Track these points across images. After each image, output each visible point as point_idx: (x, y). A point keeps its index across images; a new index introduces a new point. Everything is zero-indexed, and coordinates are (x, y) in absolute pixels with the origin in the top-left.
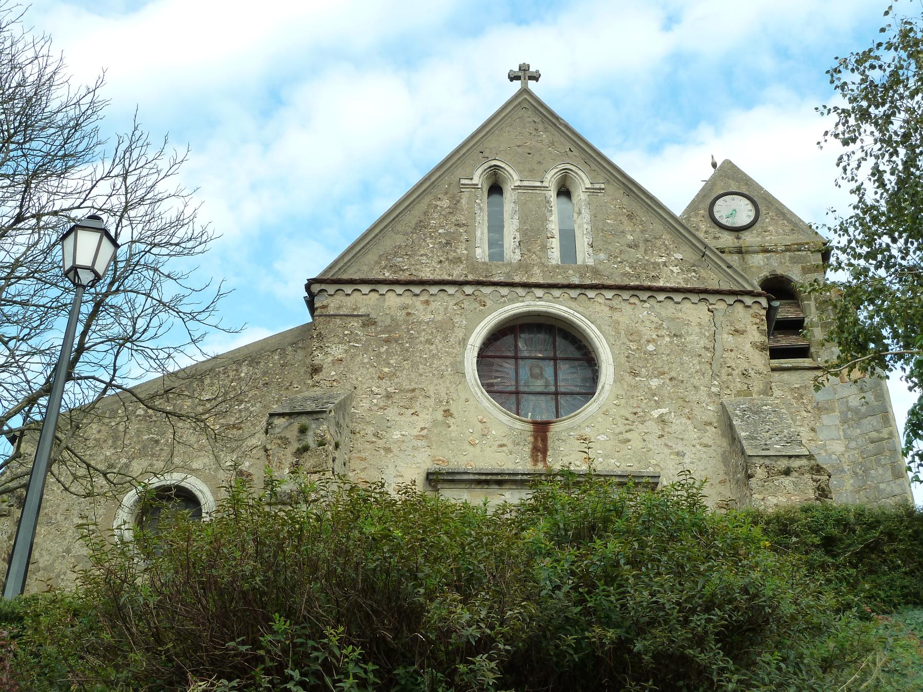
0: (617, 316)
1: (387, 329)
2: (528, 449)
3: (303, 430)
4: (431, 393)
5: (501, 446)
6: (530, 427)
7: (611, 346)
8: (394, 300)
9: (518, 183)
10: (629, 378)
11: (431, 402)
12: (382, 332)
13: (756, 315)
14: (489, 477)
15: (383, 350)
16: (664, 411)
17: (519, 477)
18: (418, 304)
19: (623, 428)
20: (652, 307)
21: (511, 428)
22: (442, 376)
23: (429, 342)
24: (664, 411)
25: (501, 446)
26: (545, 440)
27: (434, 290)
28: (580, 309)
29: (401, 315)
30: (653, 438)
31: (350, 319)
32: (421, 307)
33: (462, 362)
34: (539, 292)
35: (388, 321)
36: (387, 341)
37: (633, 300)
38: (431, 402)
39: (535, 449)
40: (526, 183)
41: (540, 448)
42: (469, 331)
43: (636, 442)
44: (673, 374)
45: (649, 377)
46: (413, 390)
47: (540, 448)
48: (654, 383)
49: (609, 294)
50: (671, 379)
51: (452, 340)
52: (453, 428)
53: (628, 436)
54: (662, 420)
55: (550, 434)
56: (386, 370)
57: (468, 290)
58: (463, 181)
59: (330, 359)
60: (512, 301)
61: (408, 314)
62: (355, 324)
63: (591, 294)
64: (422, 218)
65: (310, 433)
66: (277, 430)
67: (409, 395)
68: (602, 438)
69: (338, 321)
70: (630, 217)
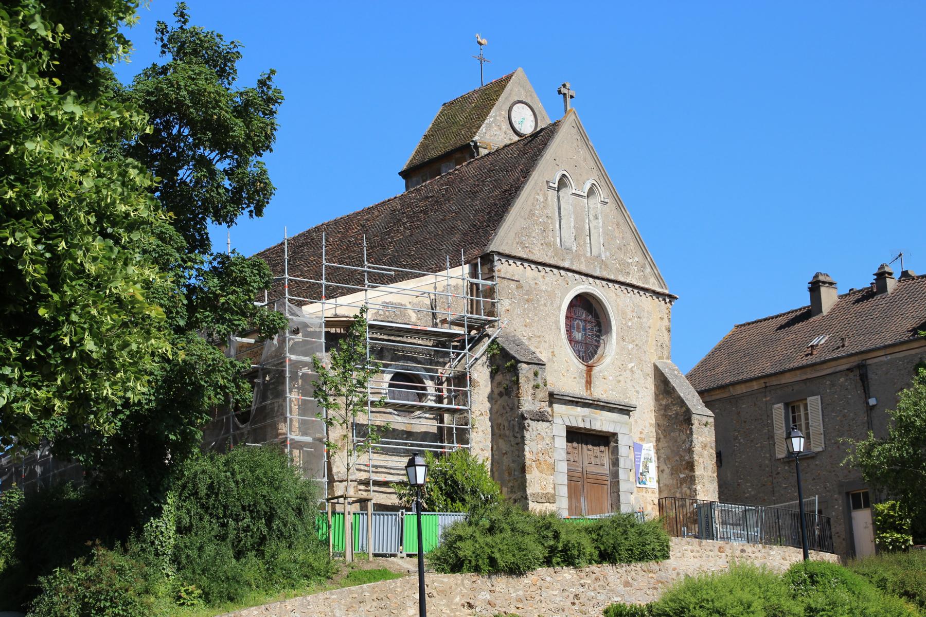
0: (618, 300)
1: (528, 293)
2: (584, 381)
3: (536, 374)
4: (547, 339)
5: (575, 378)
6: (585, 368)
7: (616, 320)
8: (529, 273)
9: (574, 191)
10: (621, 342)
11: (546, 345)
12: (526, 294)
13: (668, 308)
14: (580, 400)
15: (527, 306)
16: (633, 364)
17: (587, 401)
18: (540, 277)
19: (618, 374)
20: (631, 297)
21: (578, 368)
22: (551, 330)
23: (545, 305)
24: (633, 364)
25: (575, 378)
26: (590, 377)
27: (548, 269)
28: (605, 294)
29: (532, 283)
30: (628, 381)
31: (511, 282)
32: (541, 280)
33: (559, 321)
34: (591, 280)
35: (527, 288)
36: (528, 301)
37: (625, 291)
38: (546, 345)
39: (587, 382)
40: (577, 192)
41: (589, 383)
42: (562, 299)
43: (622, 383)
44: (637, 342)
45: (629, 343)
46: (539, 337)
47: (589, 383)
48: (630, 346)
49: (617, 286)
50: (637, 345)
51: (555, 306)
52: (556, 364)
53: (620, 378)
54: (632, 371)
55: (592, 373)
56: (528, 321)
57: (562, 272)
58: (551, 185)
59: (504, 309)
60: (579, 284)
61: (536, 284)
62: (513, 285)
63: (610, 285)
64: (532, 207)
65: (539, 376)
66: (524, 372)
67: (538, 339)
68: (611, 378)
69: (505, 282)
70: (618, 225)
